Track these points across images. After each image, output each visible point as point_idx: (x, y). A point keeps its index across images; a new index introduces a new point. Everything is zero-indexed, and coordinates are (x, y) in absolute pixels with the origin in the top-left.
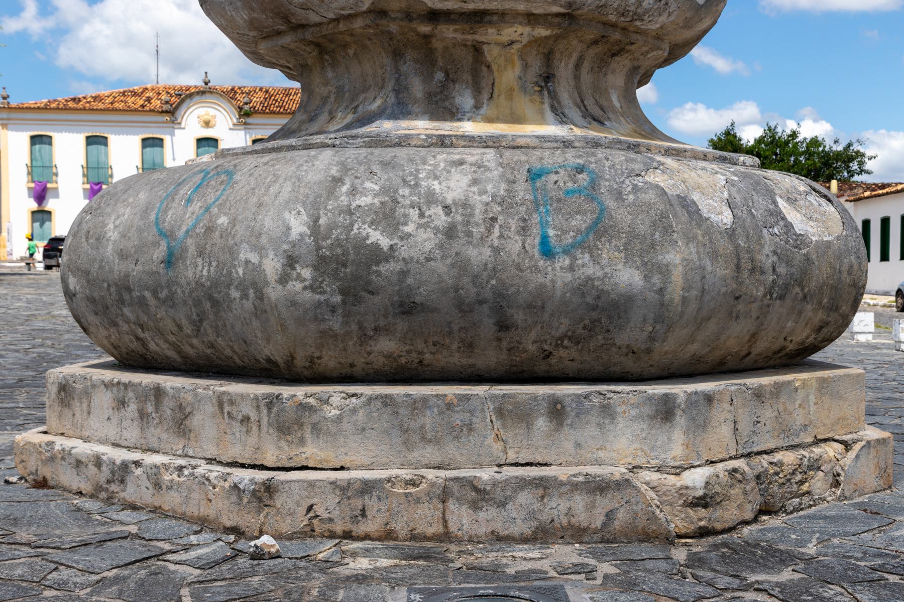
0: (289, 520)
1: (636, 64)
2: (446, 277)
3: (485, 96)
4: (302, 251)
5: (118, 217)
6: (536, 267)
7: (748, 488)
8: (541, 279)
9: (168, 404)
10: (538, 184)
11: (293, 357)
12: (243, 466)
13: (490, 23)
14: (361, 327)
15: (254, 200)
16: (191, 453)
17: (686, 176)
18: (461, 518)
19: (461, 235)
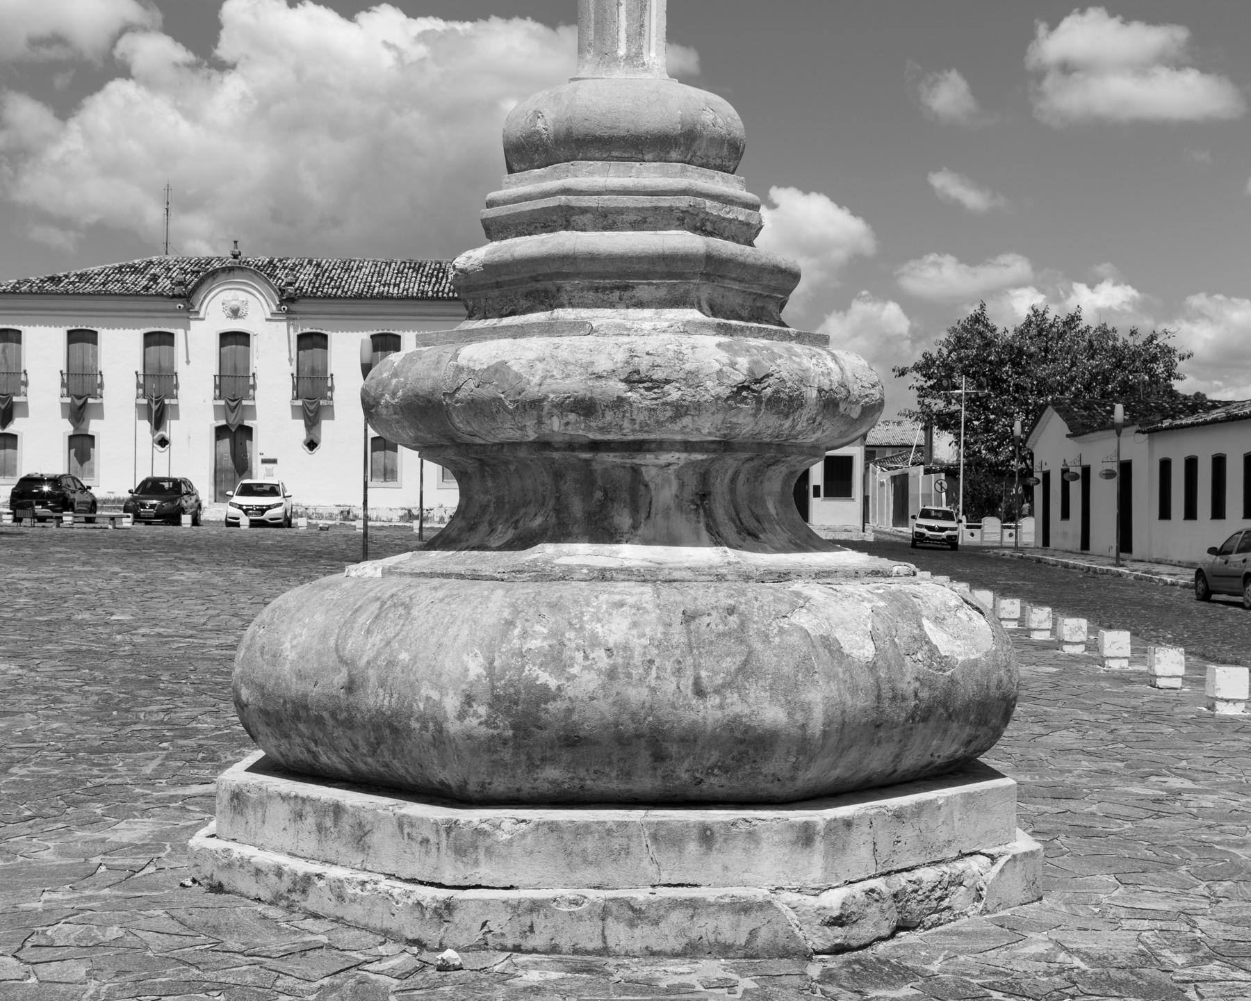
0: (466, 934)
1: (792, 469)
2: (607, 714)
3: (643, 515)
4: (478, 690)
5: (295, 637)
6: (689, 705)
8: (693, 716)
9: (346, 822)
10: (692, 627)
11: (466, 783)
12: (421, 883)
13: (649, 451)
14: (529, 758)
15: (433, 640)
16: (369, 868)
17: (831, 611)
18: (619, 935)
19: (622, 676)
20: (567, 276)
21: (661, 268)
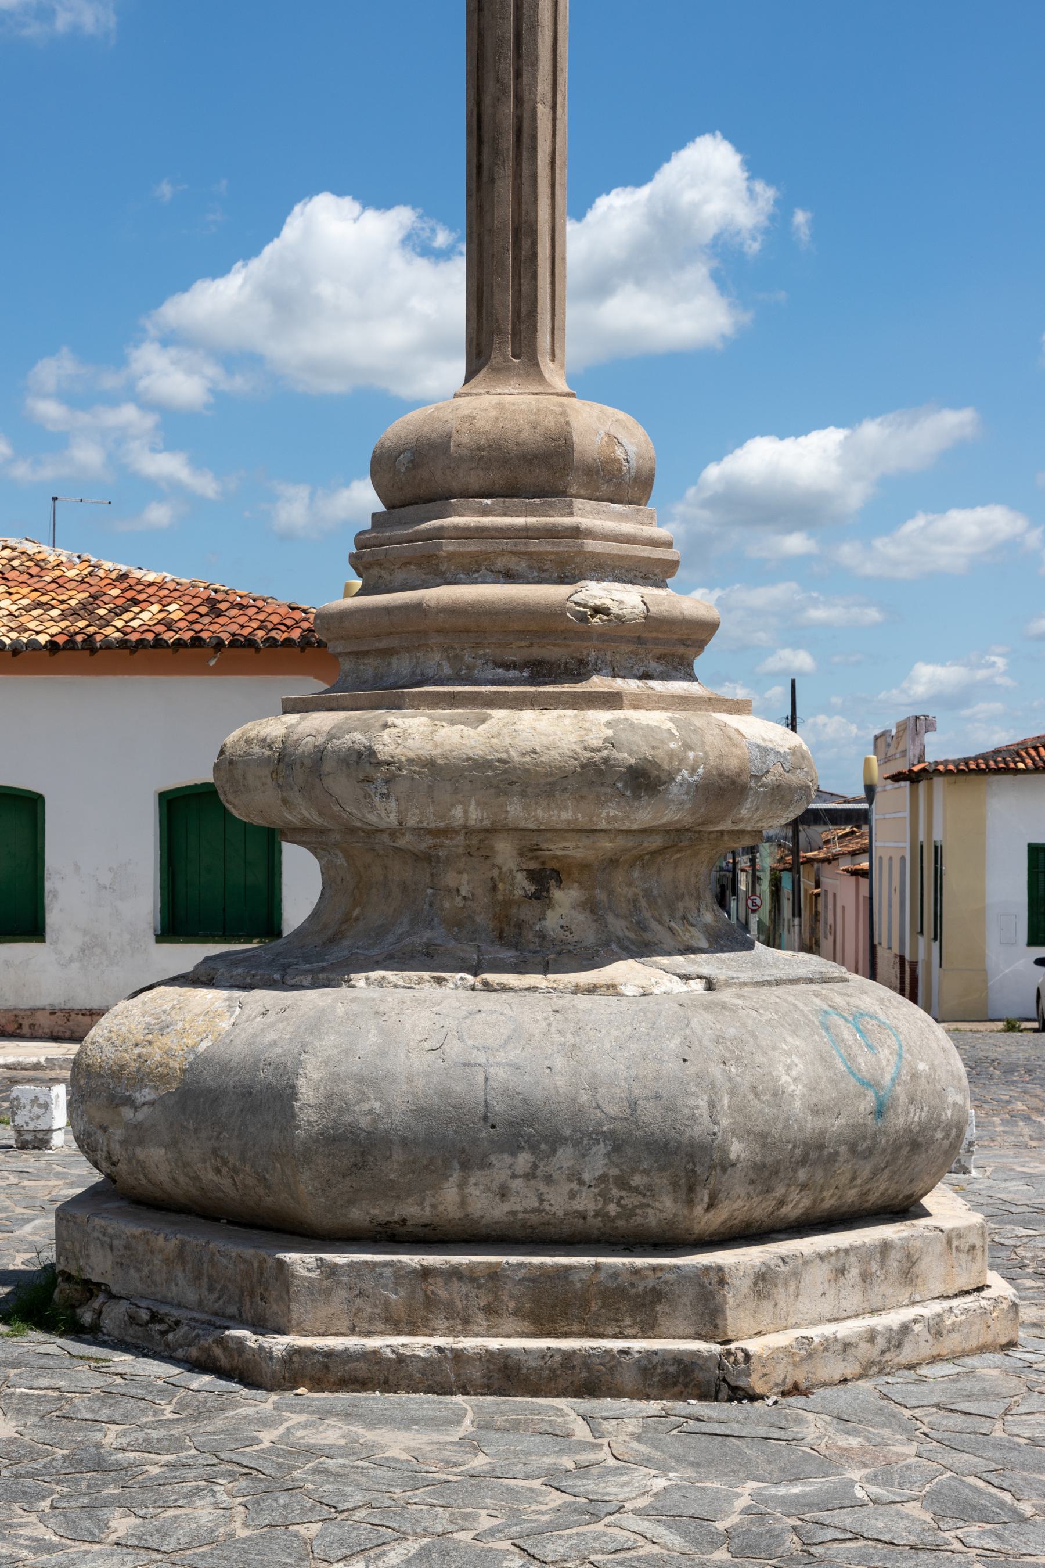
9: (894, 1256)
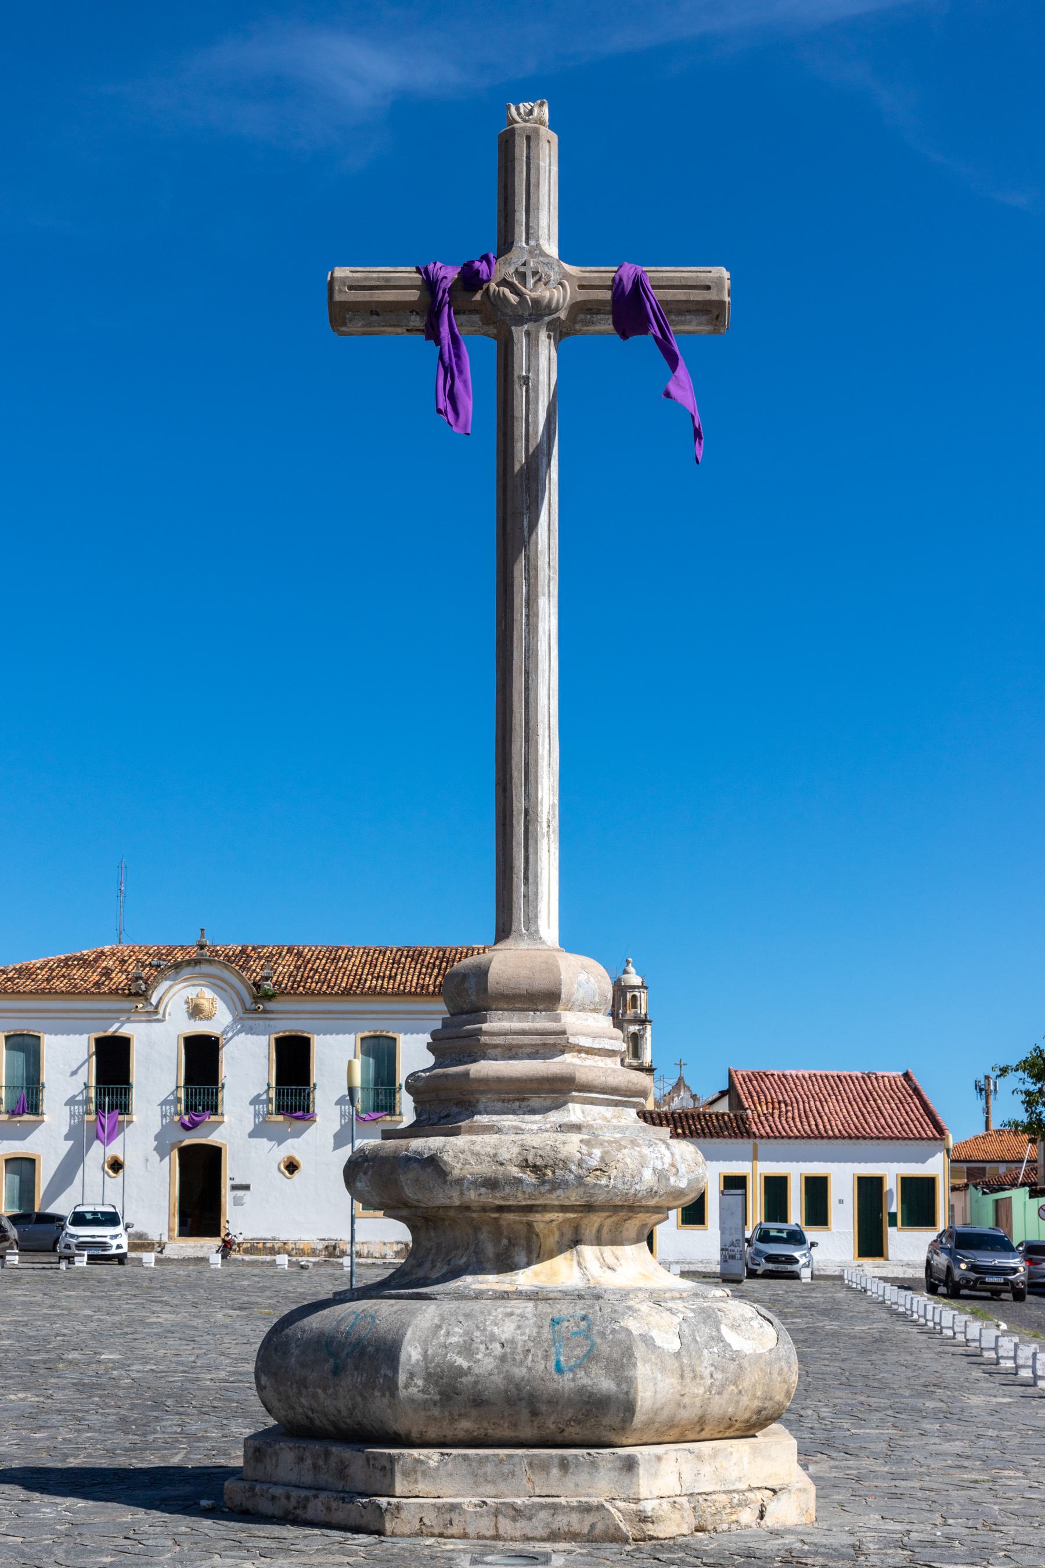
3: (535, 1255)
4: (416, 1370)
7: (685, 1514)
8: (556, 1386)
11: (410, 1432)
13: (537, 1212)
14: (451, 1414)
18: (506, 1526)
20: (482, 1092)
21: (546, 1086)
